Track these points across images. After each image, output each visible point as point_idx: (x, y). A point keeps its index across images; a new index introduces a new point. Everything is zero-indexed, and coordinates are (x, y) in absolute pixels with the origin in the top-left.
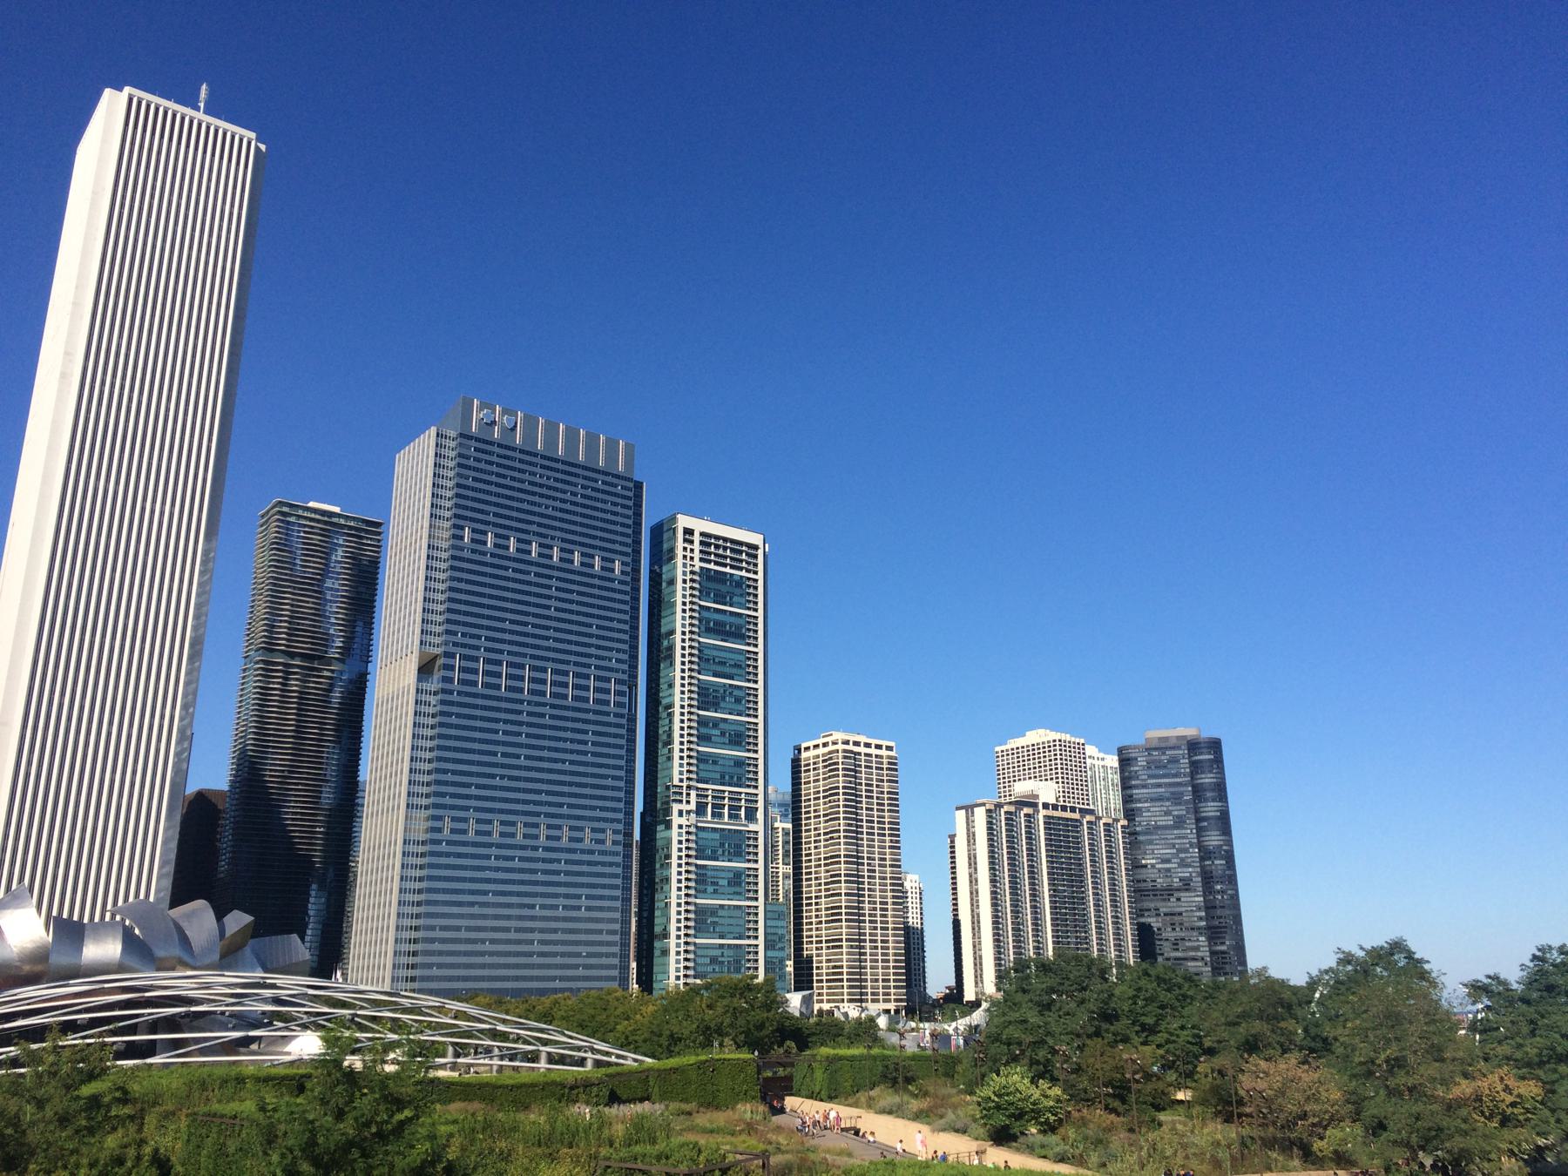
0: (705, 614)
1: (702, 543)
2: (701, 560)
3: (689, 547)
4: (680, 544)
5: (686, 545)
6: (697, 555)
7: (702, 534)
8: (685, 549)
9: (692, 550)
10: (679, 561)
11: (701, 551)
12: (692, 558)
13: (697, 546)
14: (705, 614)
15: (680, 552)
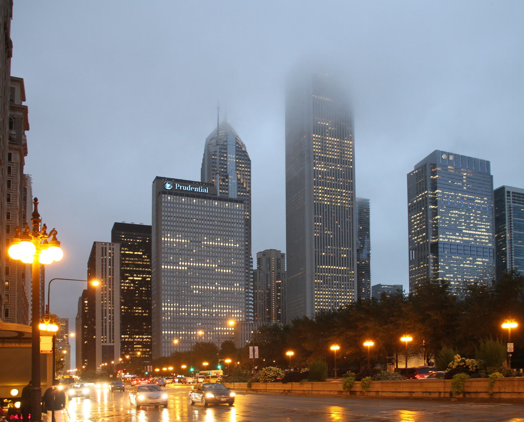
0: (515, 222)
1: (513, 196)
2: (513, 202)
3: (509, 198)
4: (506, 197)
5: (508, 197)
6: (511, 201)
7: (513, 193)
8: (508, 199)
9: (510, 199)
10: (506, 204)
11: (513, 199)
12: (510, 202)
13: (511, 197)
14: (515, 222)
15: (506, 201)
